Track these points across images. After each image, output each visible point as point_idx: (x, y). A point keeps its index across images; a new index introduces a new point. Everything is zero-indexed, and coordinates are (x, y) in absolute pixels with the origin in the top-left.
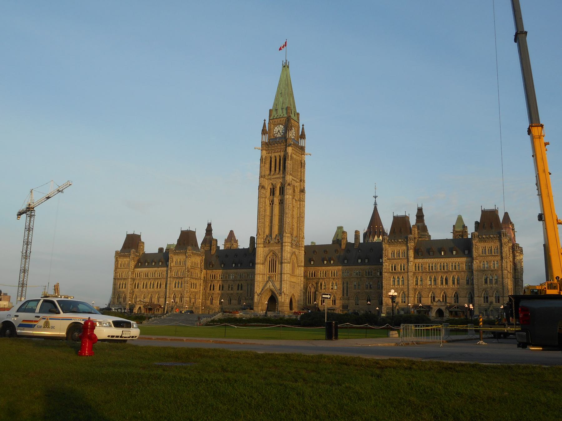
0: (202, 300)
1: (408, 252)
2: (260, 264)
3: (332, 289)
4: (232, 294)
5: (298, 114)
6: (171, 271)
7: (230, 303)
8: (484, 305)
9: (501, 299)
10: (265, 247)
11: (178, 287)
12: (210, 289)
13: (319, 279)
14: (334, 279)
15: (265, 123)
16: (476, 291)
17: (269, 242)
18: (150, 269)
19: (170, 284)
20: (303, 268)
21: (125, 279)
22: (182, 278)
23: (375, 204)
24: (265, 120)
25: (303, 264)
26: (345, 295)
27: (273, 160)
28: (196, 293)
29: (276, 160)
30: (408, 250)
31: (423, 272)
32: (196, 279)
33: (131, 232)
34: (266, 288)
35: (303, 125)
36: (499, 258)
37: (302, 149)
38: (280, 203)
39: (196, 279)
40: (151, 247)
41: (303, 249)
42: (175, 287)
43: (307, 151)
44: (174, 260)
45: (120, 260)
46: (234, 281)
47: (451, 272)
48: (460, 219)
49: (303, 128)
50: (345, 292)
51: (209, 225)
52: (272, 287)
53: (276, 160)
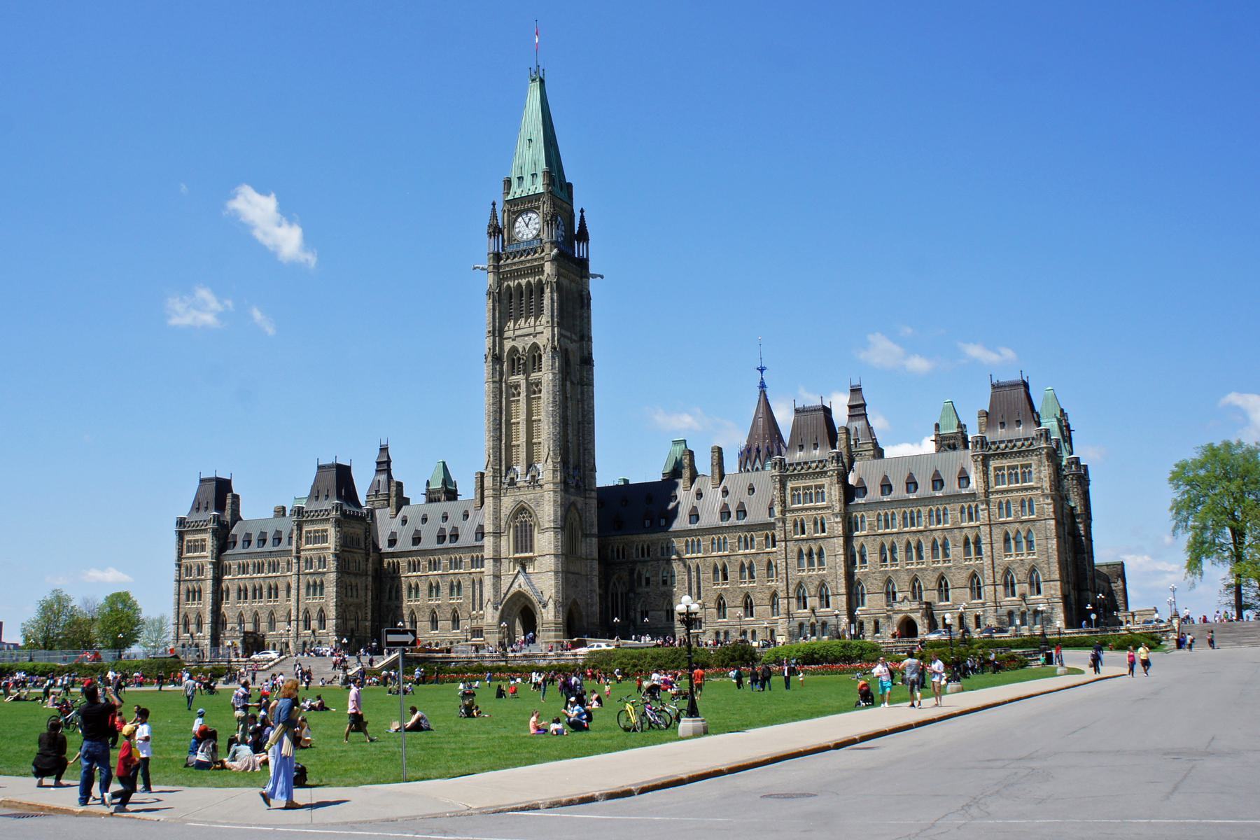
0: (373, 621)
5: (570, 186)
6: (298, 558)
8: (1008, 601)
12: (390, 598)
13: (635, 562)
15: (494, 210)
16: (988, 572)
17: (512, 483)
20: (595, 540)
22: (324, 573)
23: (763, 386)
24: (494, 204)
25: (595, 530)
28: (358, 606)
30: (831, 484)
34: (512, 591)
35: (582, 211)
37: (583, 264)
39: (356, 575)
40: (255, 509)
41: (594, 494)
43: (591, 271)
49: (582, 218)
51: (384, 450)
52: (526, 588)
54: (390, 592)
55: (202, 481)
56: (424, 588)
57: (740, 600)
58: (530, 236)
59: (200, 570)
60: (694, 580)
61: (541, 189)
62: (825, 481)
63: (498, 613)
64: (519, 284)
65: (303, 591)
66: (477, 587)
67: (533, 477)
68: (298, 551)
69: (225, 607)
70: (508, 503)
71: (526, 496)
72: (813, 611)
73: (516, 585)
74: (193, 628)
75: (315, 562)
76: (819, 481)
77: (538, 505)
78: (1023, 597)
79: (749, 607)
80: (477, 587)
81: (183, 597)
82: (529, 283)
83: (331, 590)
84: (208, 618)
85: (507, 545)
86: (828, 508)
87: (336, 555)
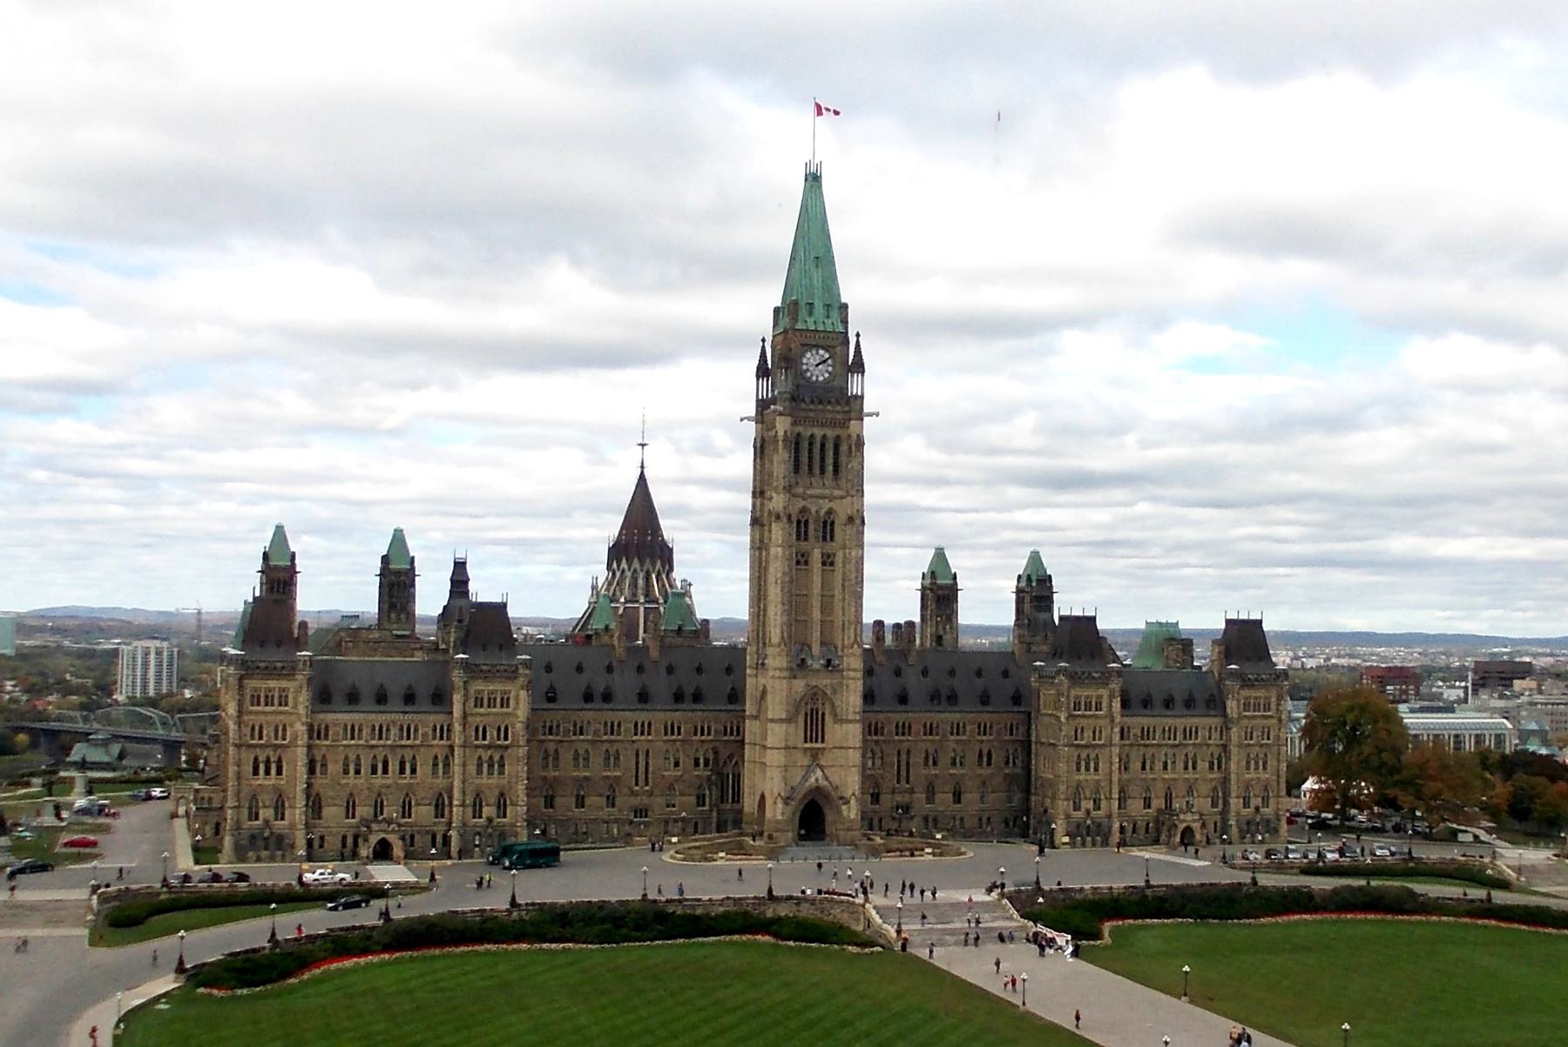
2: (788, 721)
4: (587, 778)
7: (580, 802)
9: (1271, 801)
11: (490, 773)
14: (877, 742)
18: (373, 716)
19: (464, 765)
21: (277, 747)
22: (507, 747)
26: (903, 781)
29: (811, 444)
30: (1111, 697)
36: (1275, 721)
38: (824, 564)
42: (479, 772)
44: (472, 691)
45: (252, 684)
46: (593, 742)
50: (903, 773)
56: (567, 756)
57: (950, 787)
59: (281, 730)
60: (903, 763)
62: (1104, 692)
63: (789, 810)
65: (472, 769)
66: (642, 758)
67: (829, 661)
68: (465, 716)
69: (319, 782)
70: (799, 685)
71: (824, 681)
72: (1088, 812)
74: (266, 813)
75: (491, 733)
76: (1102, 691)
77: (835, 691)
78: (1257, 809)
79: (957, 797)
80: (642, 758)
84: (300, 801)
85: (796, 733)
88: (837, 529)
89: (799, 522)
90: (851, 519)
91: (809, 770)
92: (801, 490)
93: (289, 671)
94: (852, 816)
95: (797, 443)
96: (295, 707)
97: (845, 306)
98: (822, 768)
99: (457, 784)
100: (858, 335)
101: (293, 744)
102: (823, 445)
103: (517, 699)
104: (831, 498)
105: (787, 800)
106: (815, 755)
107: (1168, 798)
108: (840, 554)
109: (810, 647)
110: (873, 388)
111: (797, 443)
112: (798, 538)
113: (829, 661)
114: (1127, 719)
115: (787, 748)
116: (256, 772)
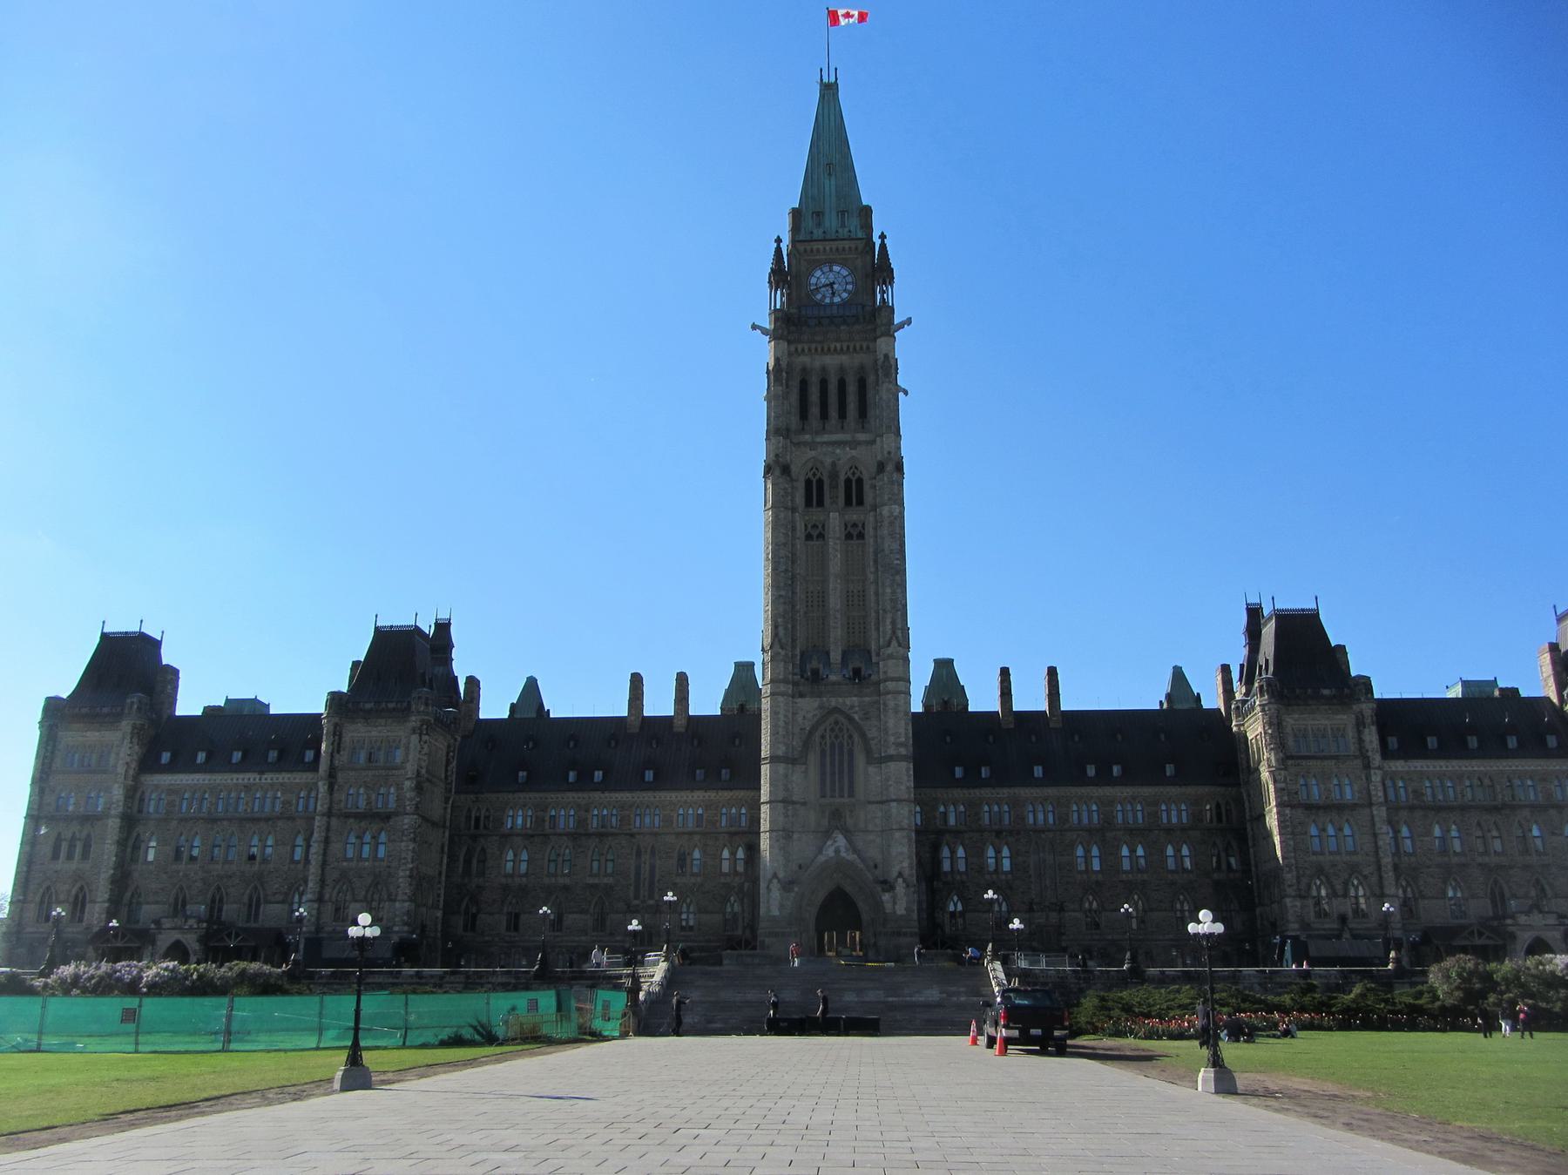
1: (1359, 732)
3: (996, 871)
10: (802, 695)
13: (940, 833)
14: (998, 833)
17: (816, 678)
19: (327, 841)
22: (387, 817)
24: (779, 240)
27: (814, 381)
29: (824, 383)
30: (1360, 724)
31: (1412, 808)
32: (434, 824)
33: (117, 626)
34: (821, 858)
38: (849, 536)
39: (434, 824)
44: (347, 738)
47: (1513, 808)
48: (1178, 676)
51: (443, 628)
53: (824, 383)
54: (468, 862)
55: (104, 636)
58: (837, 300)
61: (860, 235)
62: (1345, 719)
64: (824, 369)
67: (857, 672)
68: (332, 774)
73: (830, 852)
77: (866, 717)
81: (46, 850)
82: (842, 369)
83: (406, 847)
85: (805, 782)
86: (1356, 757)
87: (419, 788)
88: (866, 487)
89: (808, 483)
90: (881, 467)
91: (828, 834)
92: (807, 437)
93: (114, 719)
94: (901, 910)
95: (804, 385)
96: (115, 767)
97: (867, 211)
98: (847, 833)
99: (314, 869)
100: (883, 237)
101: (104, 816)
102: (842, 384)
103: (407, 748)
104: (854, 444)
105: (787, 886)
106: (836, 814)
107: (1498, 899)
108: (871, 518)
109: (828, 653)
110: (903, 297)
111: (804, 385)
112: (808, 503)
113: (857, 672)
114: (1398, 765)
115: (783, 801)
116: (55, 856)
